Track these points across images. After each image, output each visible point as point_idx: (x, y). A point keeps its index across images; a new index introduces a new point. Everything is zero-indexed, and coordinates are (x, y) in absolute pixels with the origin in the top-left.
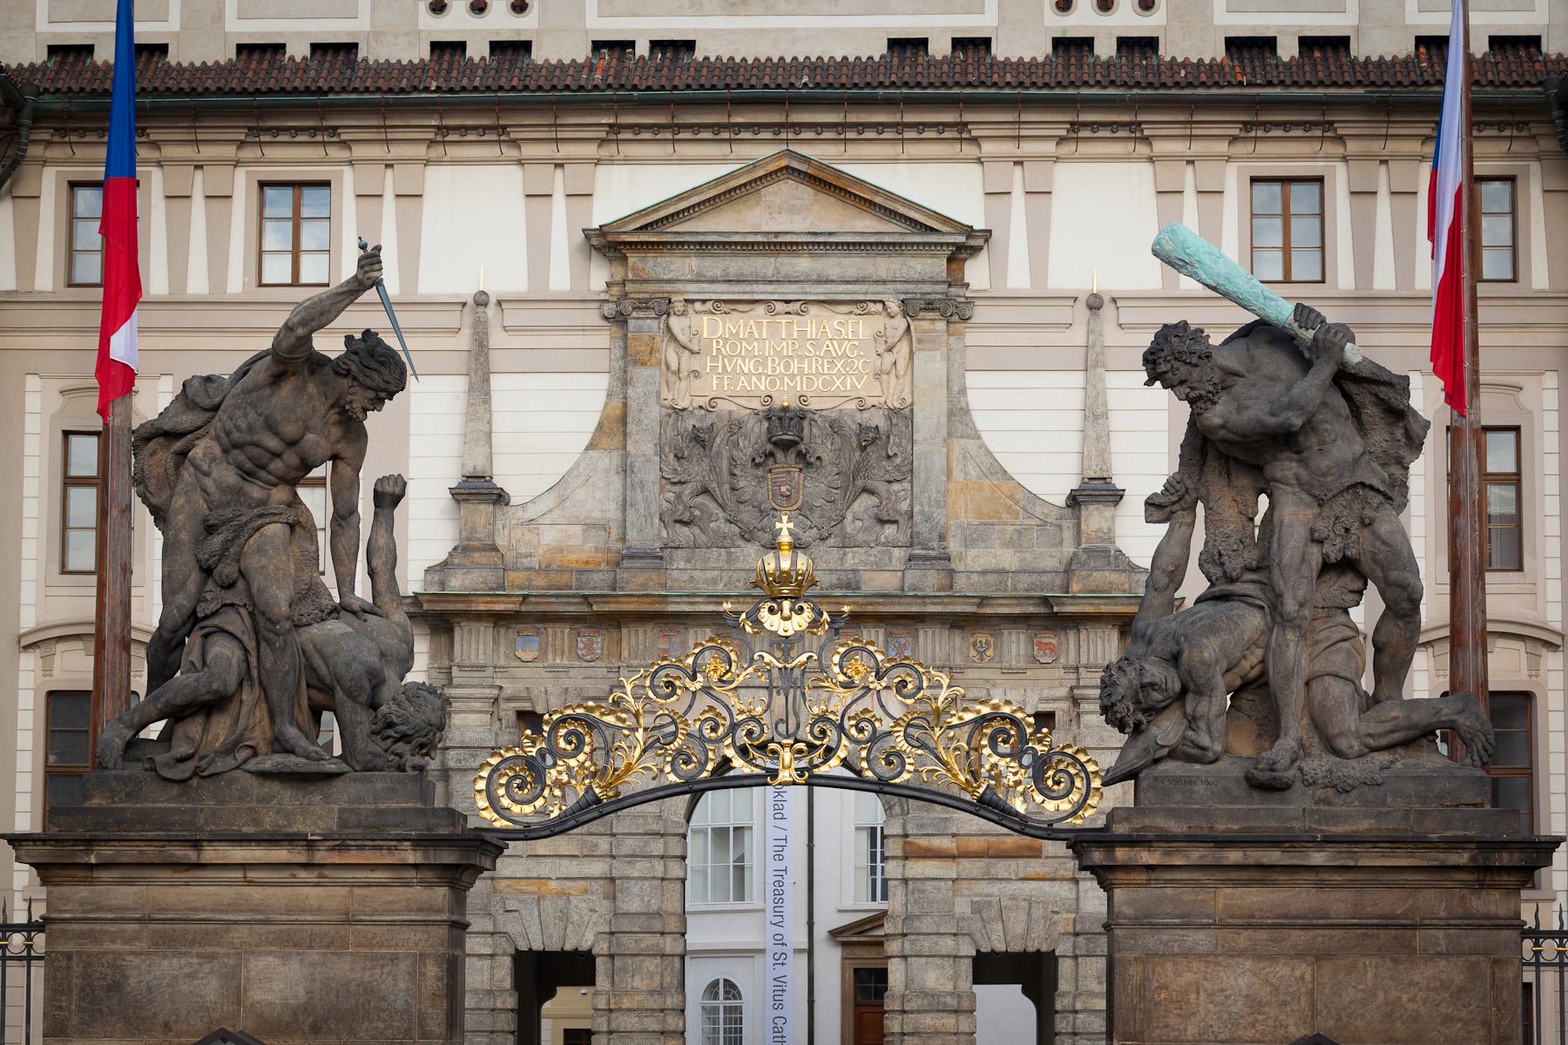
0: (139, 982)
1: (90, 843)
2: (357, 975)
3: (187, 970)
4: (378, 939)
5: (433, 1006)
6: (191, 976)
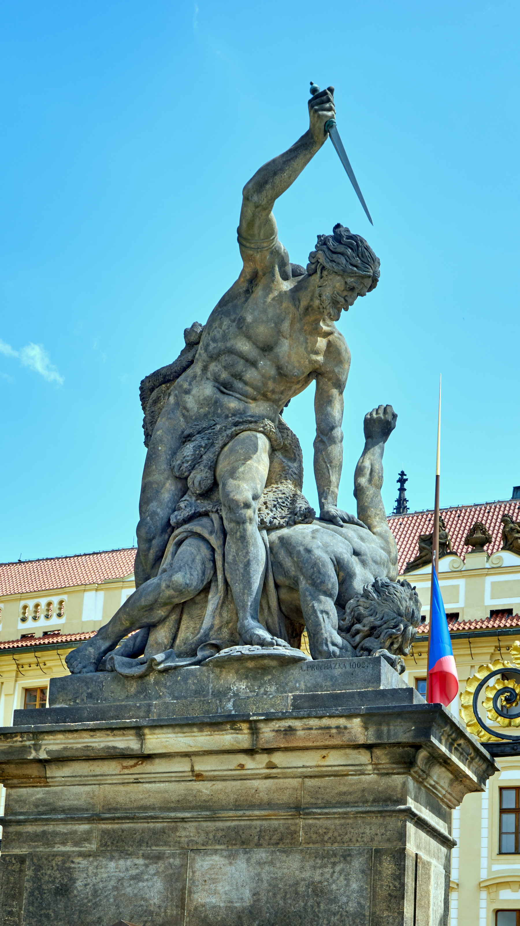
0: (86, 885)
1: (37, 734)
2: (306, 875)
3: (134, 872)
4: (330, 835)
5: (388, 908)
6: (137, 878)
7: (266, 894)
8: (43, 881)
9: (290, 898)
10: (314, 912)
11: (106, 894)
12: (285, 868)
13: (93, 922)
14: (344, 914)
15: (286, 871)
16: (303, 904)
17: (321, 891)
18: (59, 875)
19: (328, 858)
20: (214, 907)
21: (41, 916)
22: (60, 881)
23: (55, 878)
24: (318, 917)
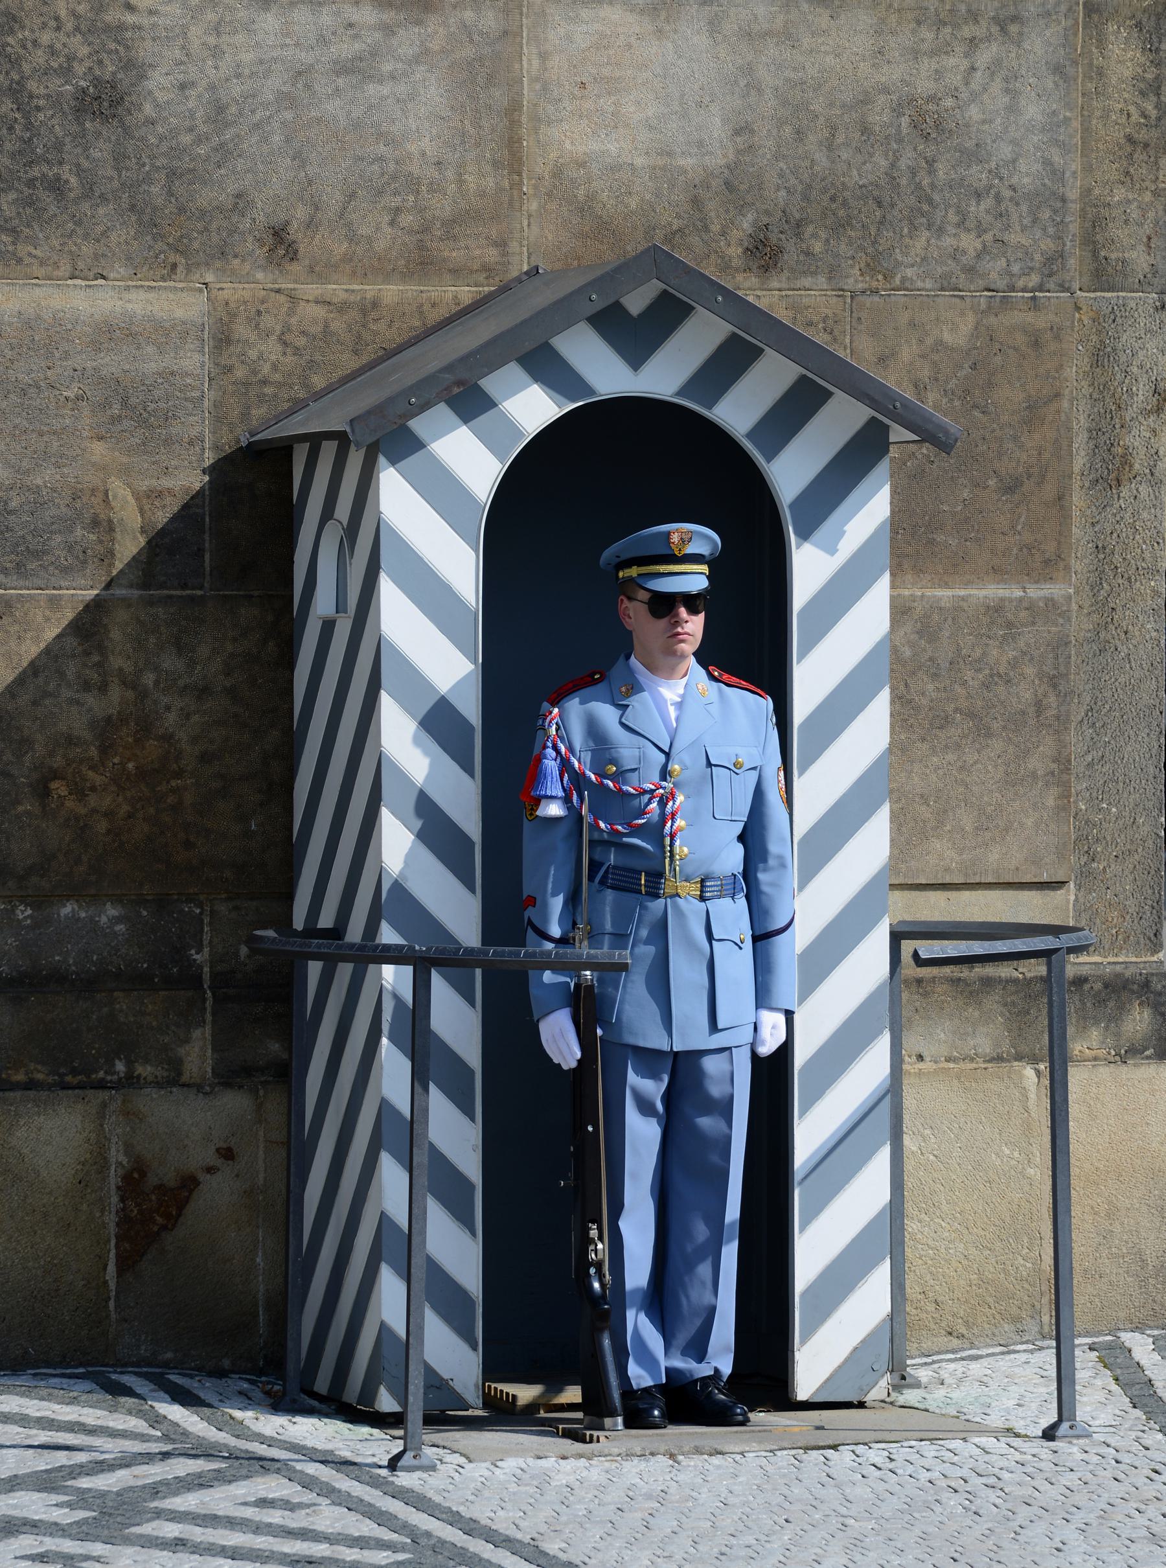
0: (183, 87)
2: (892, 74)
3: (345, 49)
7: (775, 132)
8: (26, 68)
9: (847, 144)
10: (919, 186)
11: (258, 116)
12: (826, 53)
13: (219, 208)
14: (1007, 193)
15: (830, 60)
16: (883, 163)
17: (937, 125)
18: (84, 51)
19: (956, 26)
20: (614, 168)
21: (31, 183)
22: (90, 69)
23: (71, 58)
24: (930, 202)
